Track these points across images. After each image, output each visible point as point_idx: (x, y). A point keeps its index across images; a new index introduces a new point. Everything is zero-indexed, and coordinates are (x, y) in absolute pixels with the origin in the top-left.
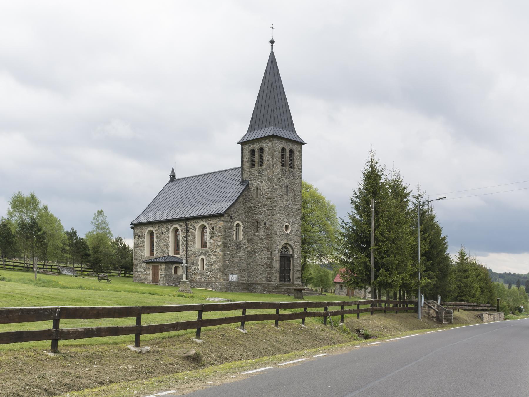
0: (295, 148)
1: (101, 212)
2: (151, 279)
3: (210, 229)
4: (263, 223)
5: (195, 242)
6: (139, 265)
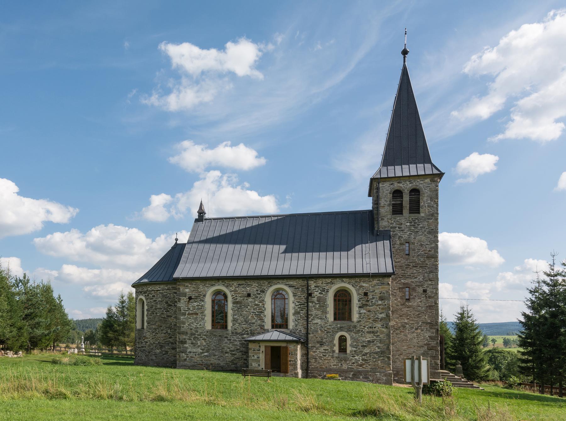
2: (263, 366)
3: (359, 294)
4: (420, 290)
5: (325, 312)
6: (188, 341)
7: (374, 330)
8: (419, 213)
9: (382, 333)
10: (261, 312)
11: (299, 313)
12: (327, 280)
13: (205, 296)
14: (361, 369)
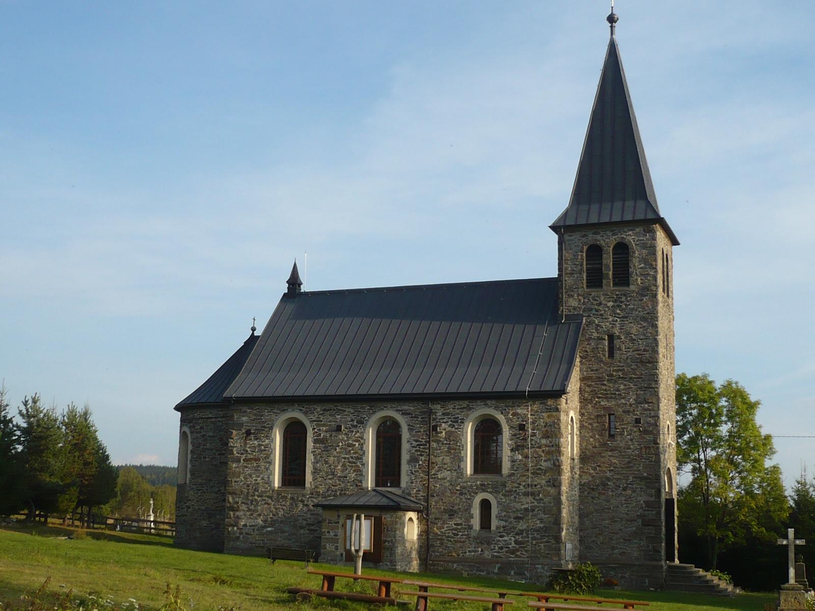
3: (511, 428)
7: (535, 489)
9: (547, 494)
10: (358, 458)
11: (417, 460)
12: (461, 403)
14: (512, 558)
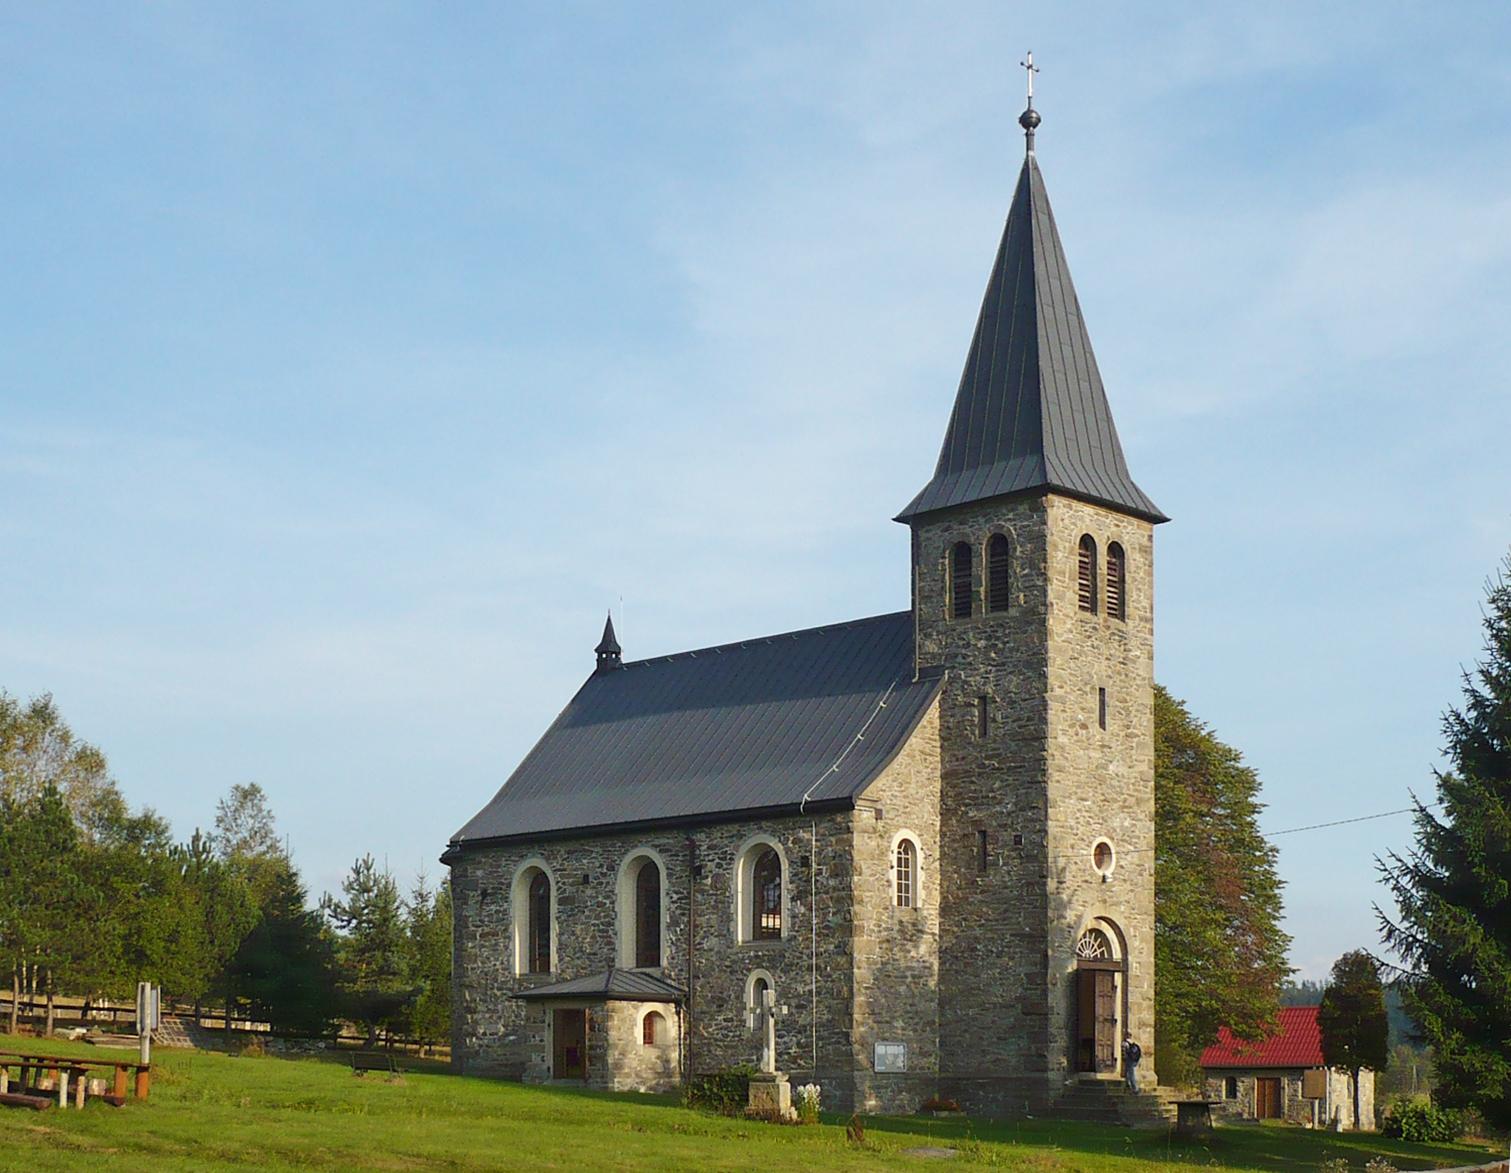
0: (1130, 532)
1: (248, 794)
2: (550, 1062)
3: (791, 863)
4: (1007, 836)
8: (1006, 609)
12: (730, 827)
13: (509, 885)
